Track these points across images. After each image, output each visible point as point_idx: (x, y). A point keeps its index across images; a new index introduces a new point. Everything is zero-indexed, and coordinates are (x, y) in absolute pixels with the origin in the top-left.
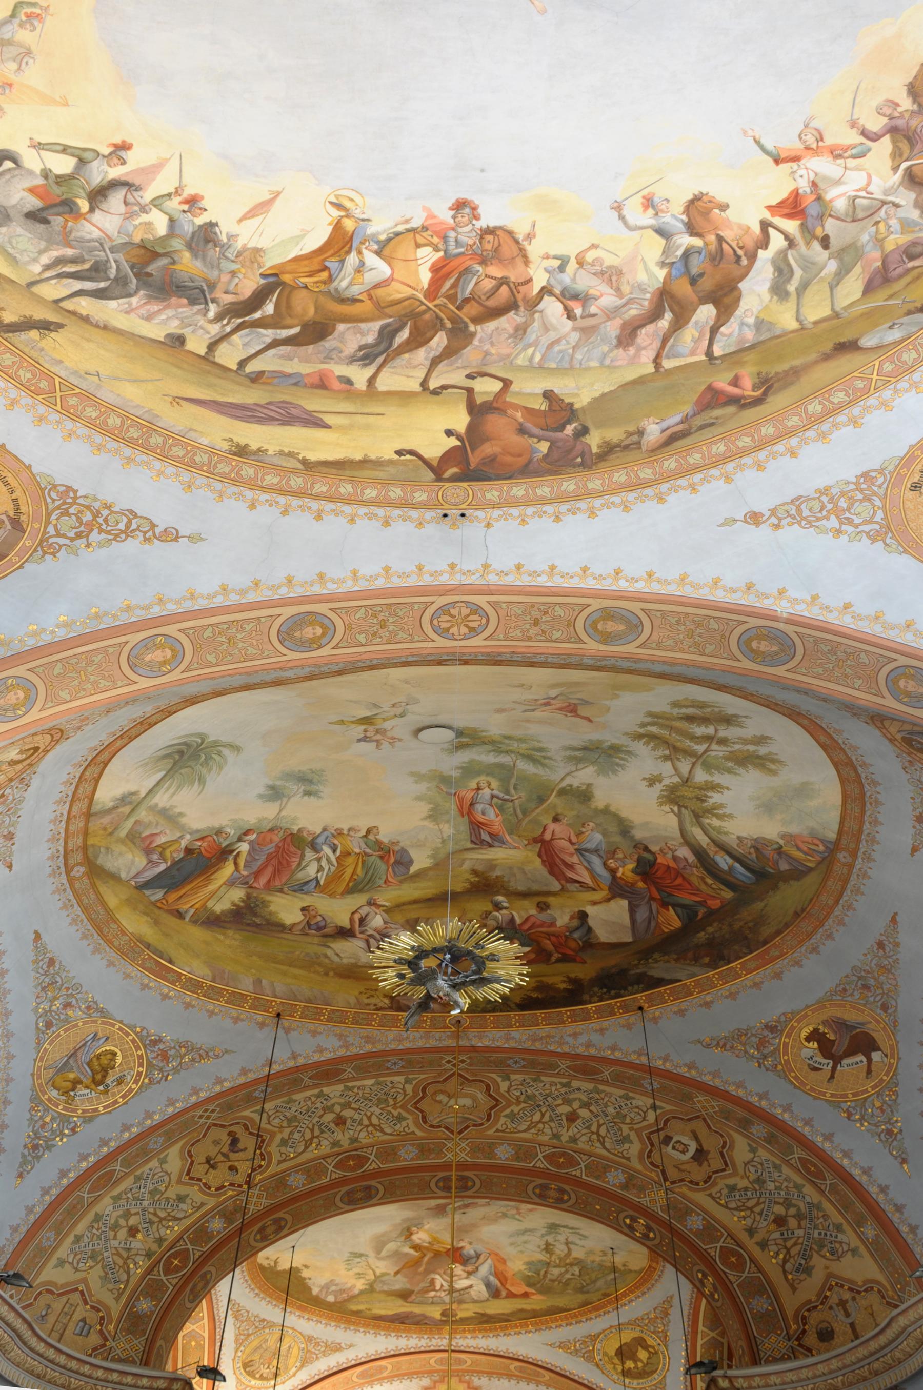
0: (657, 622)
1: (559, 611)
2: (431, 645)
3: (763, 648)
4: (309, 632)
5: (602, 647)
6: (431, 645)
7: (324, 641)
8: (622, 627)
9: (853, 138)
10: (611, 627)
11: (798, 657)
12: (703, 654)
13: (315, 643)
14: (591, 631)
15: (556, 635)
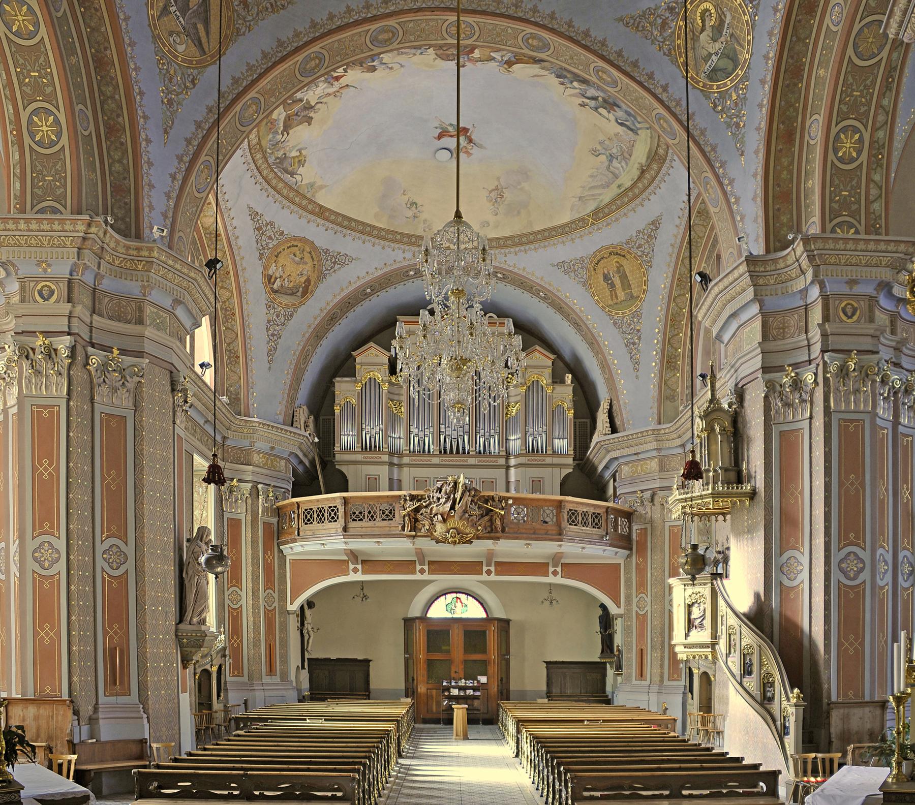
0: (364, 46)
1: (412, 38)
2: (476, 20)
3: (313, 62)
4: (535, 43)
5: (387, 23)
6: (476, 20)
7: (528, 36)
8: (380, 37)
9: (324, 100)
10: (386, 36)
11: (297, 71)
12: (339, 41)
13: (533, 36)
14: (395, 30)
15: (411, 25)
